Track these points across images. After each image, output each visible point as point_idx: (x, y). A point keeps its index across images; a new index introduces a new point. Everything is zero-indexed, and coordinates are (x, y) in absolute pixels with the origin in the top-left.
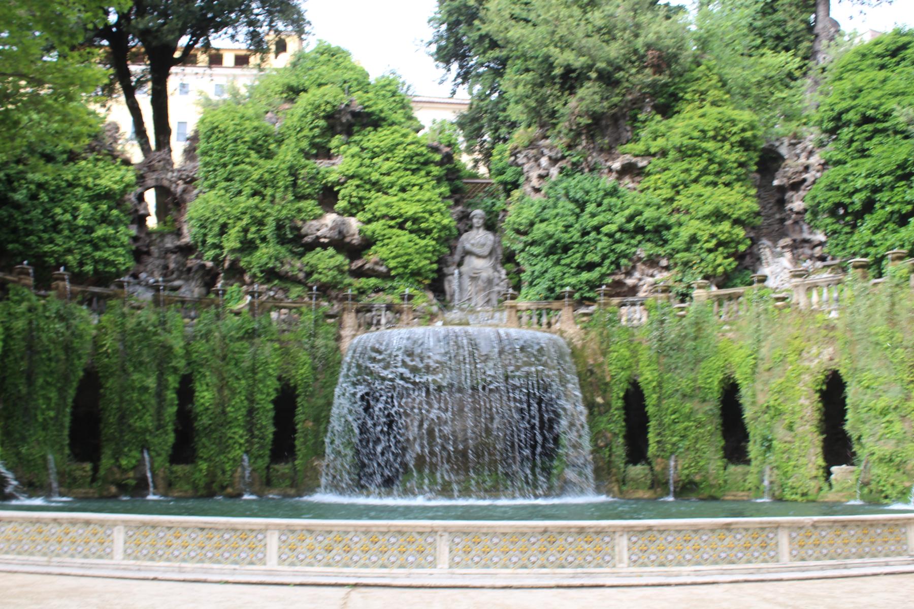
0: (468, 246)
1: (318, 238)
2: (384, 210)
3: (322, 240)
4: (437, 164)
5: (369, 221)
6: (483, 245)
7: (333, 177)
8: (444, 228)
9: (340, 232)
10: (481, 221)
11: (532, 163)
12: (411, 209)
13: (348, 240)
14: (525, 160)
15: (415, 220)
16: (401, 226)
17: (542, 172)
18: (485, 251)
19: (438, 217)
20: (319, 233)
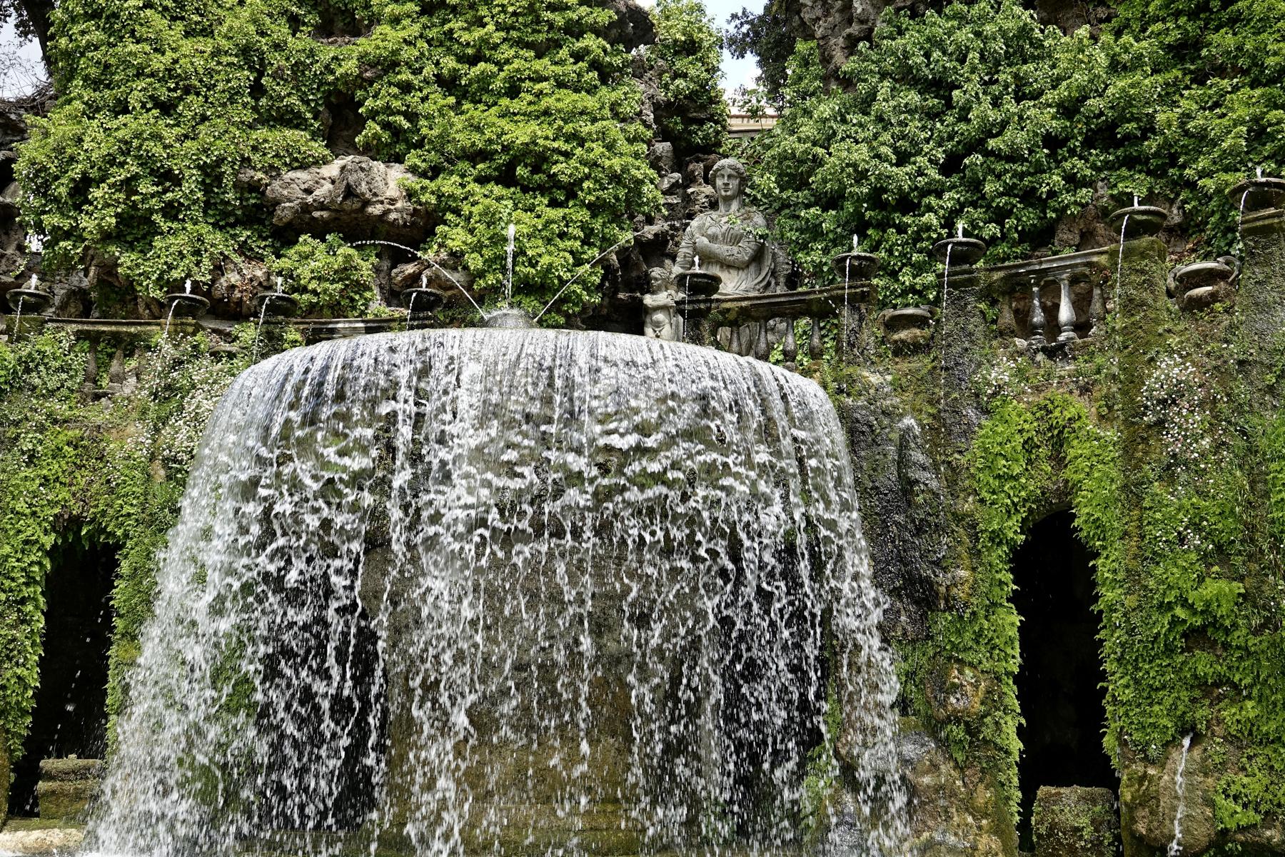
0: (703, 241)
1: (306, 208)
2: (465, 140)
3: (316, 214)
4: (598, 32)
5: (434, 172)
6: (736, 239)
7: (350, 66)
8: (616, 178)
9: (350, 192)
10: (734, 184)
11: (835, 18)
12: (520, 134)
13: (376, 210)
14: (819, 12)
15: (540, 160)
16: (506, 177)
17: (855, 29)
18: (743, 251)
19: (598, 149)
20: (310, 199)
